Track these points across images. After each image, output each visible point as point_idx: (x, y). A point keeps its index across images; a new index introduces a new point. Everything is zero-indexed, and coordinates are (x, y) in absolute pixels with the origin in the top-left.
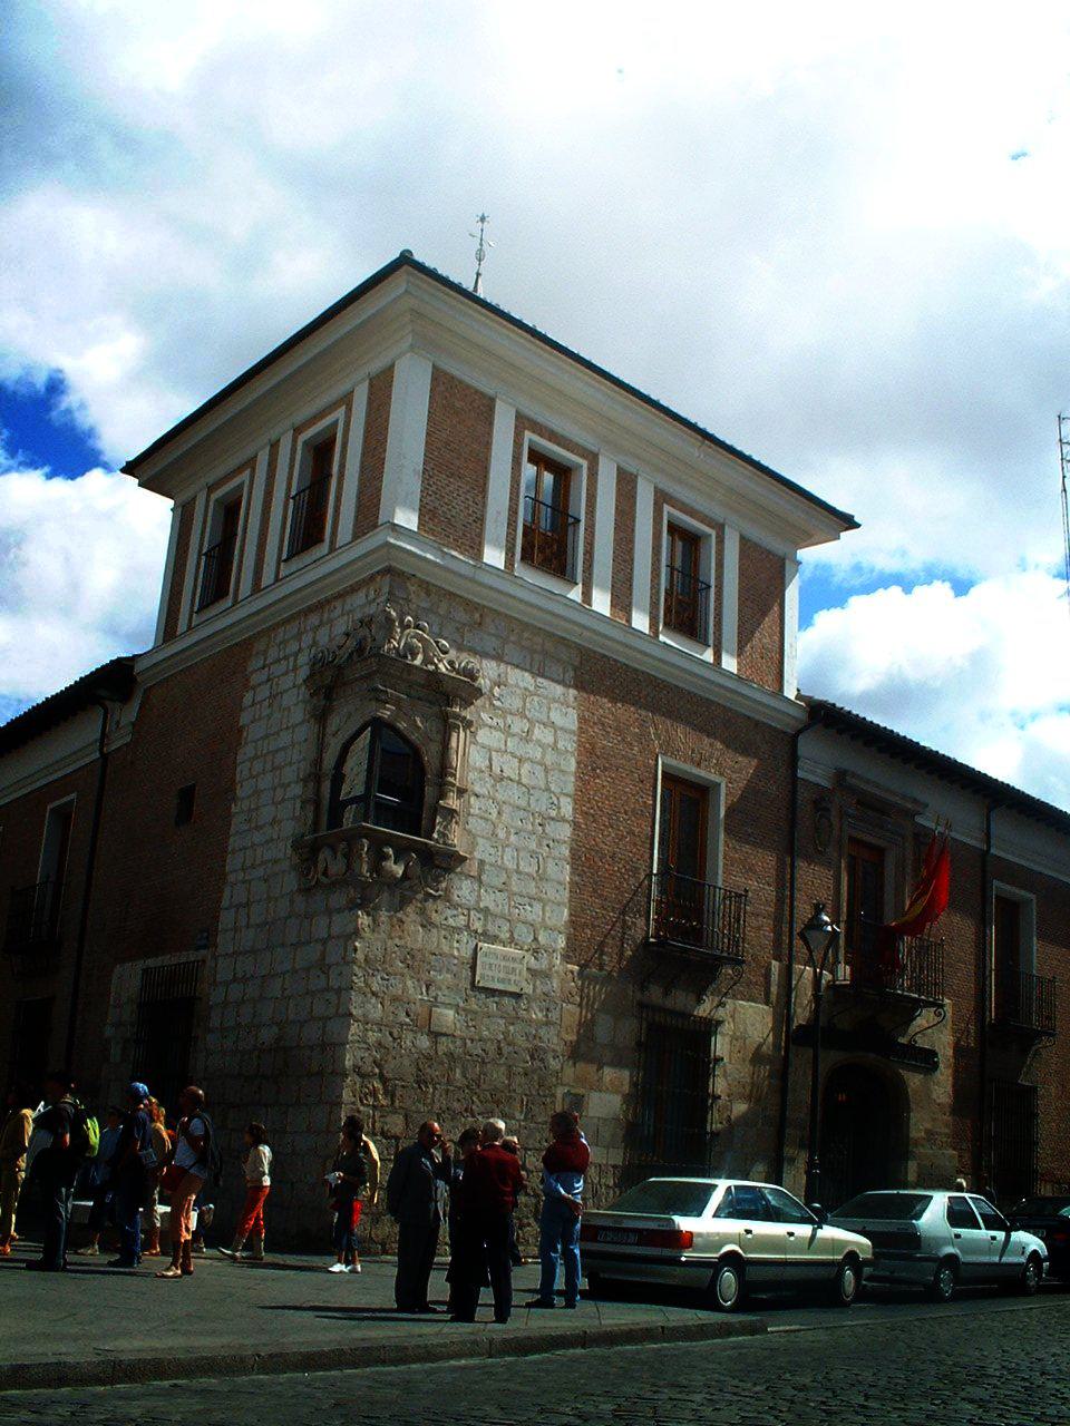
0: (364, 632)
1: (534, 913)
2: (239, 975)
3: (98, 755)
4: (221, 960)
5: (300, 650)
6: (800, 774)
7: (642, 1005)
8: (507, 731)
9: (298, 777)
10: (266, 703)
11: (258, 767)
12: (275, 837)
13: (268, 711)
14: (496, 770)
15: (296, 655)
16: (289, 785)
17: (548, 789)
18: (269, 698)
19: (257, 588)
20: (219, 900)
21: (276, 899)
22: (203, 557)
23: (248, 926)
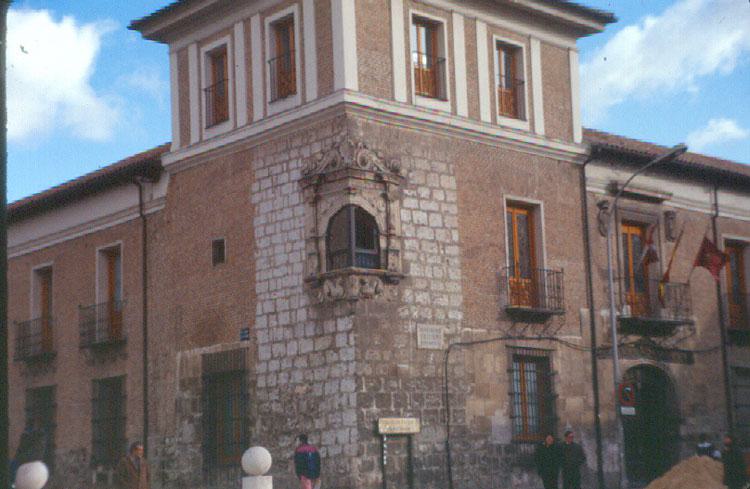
0: (333, 153)
1: (444, 301)
3: (138, 215)
6: (588, 189)
8: (419, 198)
11: (270, 230)
12: (290, 272)
14: (416, 222)
16: (295, 241)
17: (444, 227)
19: (250, 121)
20: (254, 310)
21: (296, 310)
22: (203, 93)
23: (278, 326)
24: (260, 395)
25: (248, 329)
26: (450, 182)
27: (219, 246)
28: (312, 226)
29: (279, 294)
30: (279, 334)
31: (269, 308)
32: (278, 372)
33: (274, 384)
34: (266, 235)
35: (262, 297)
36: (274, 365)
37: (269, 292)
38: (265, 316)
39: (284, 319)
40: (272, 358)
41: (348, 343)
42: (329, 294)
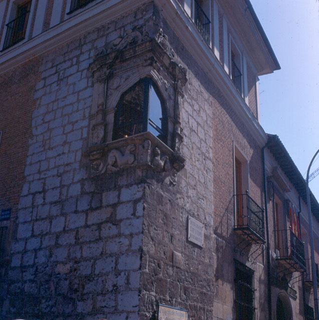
2: (37, 232)
4: (20, 226)
5: (81, 54)
9: (84, 116)
10: (55, 84)
11: (48, 117)
15: (78, 57)
16: (77, 122)
18: (57, 81)
22: (6, 27)
23: (43, 205)
24: (12, 275)
25: (10, 210)
28: (101, 100)
29: (49, 173)
30: (44, 211)
31: (36, 187)
33: (31, 262)
35: (30, 178)
36: (33, 244)
38: (31, 197)
39: (52, 196)
40: (33, 236)
41: (134, 214)
42: (115, 164)
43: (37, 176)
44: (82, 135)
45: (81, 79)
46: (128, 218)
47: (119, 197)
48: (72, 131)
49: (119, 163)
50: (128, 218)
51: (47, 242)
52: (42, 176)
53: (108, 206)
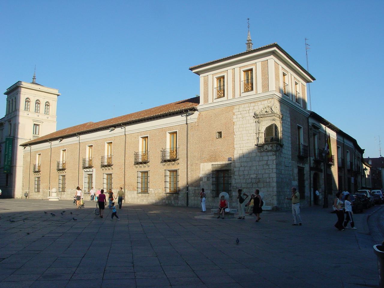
2: (242, 166)
7: (298, 166)
9: (254, 132)
11: (240, 130)
13: (242, 120)
24: (236, 177)
26: (289, 120)
27: (220, 133)
32: (243, 171)
34: (239, 131)
35: (237, 149)
36: (242, 169)
37: (240, 147)
40: (241, 166)
41: (273, 163)
43: (240, 149)
44: (254, 138)
45: (251, 119)
46: (271, 164)
47: (268, 158)
48: (250, 136)
49: (267, 149)
50: (271, 164)
51: (246, 169)
52: (242, 149)
53: (265, 160)
